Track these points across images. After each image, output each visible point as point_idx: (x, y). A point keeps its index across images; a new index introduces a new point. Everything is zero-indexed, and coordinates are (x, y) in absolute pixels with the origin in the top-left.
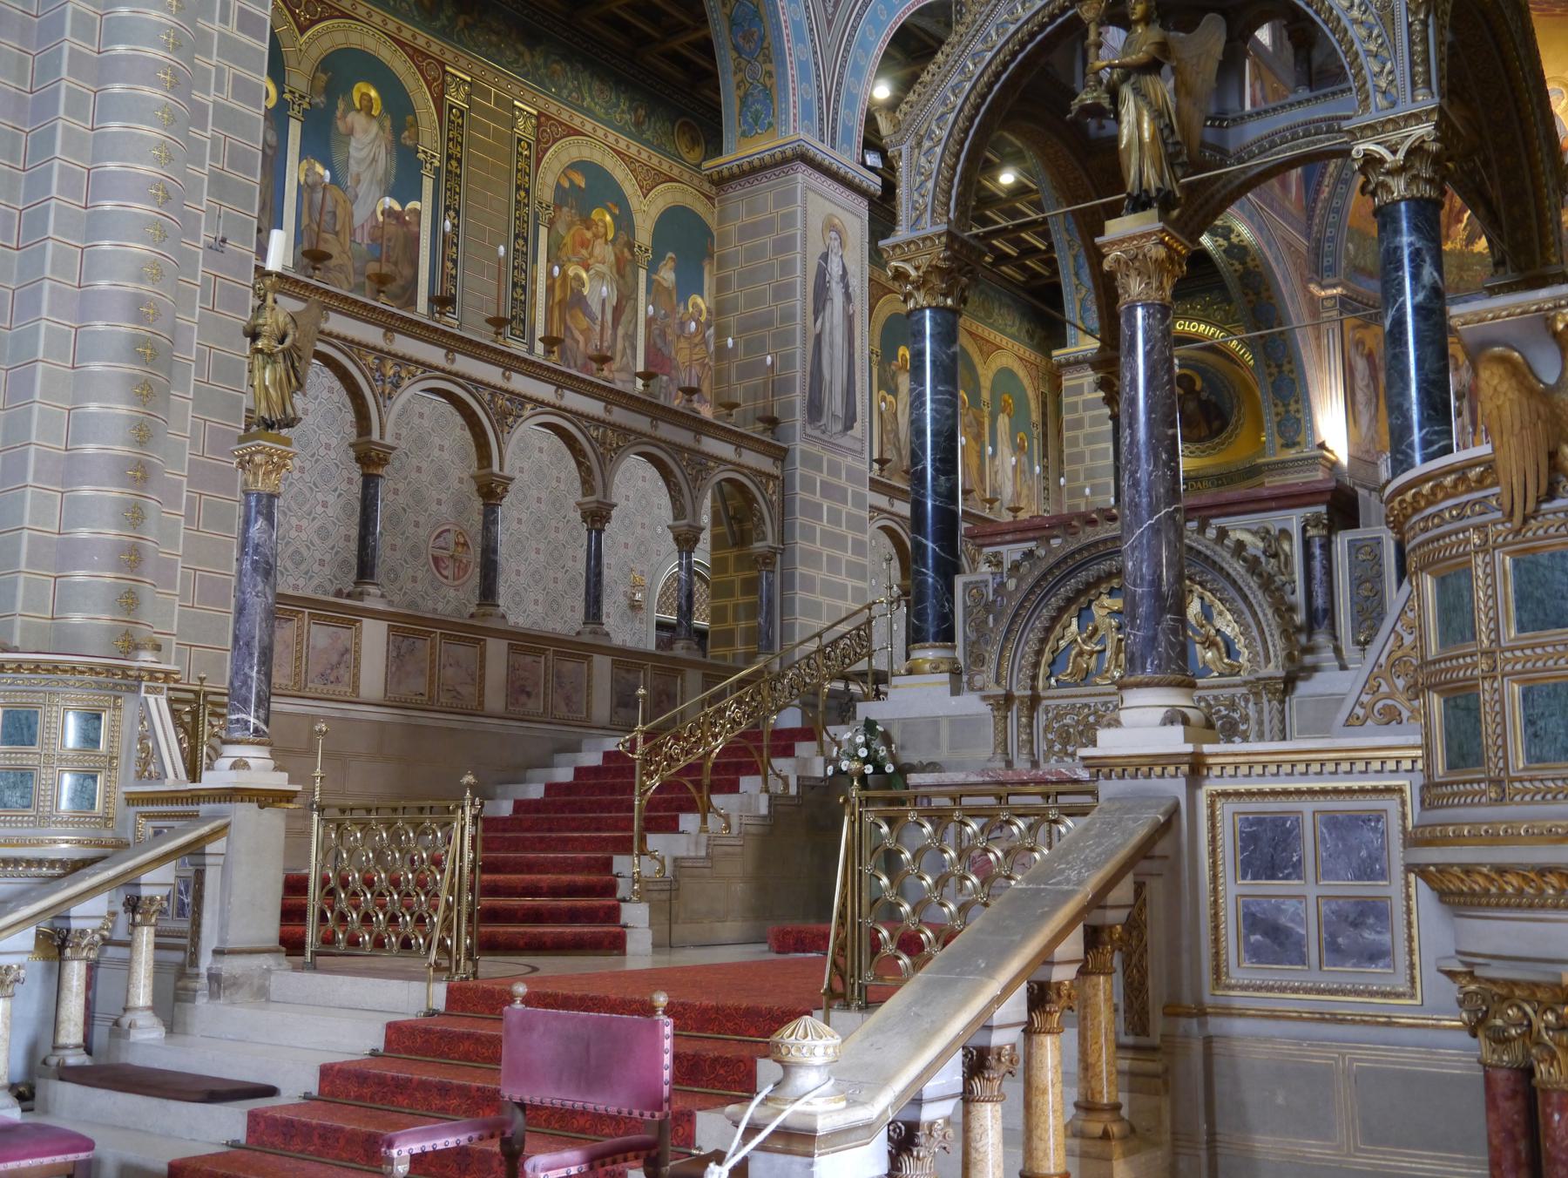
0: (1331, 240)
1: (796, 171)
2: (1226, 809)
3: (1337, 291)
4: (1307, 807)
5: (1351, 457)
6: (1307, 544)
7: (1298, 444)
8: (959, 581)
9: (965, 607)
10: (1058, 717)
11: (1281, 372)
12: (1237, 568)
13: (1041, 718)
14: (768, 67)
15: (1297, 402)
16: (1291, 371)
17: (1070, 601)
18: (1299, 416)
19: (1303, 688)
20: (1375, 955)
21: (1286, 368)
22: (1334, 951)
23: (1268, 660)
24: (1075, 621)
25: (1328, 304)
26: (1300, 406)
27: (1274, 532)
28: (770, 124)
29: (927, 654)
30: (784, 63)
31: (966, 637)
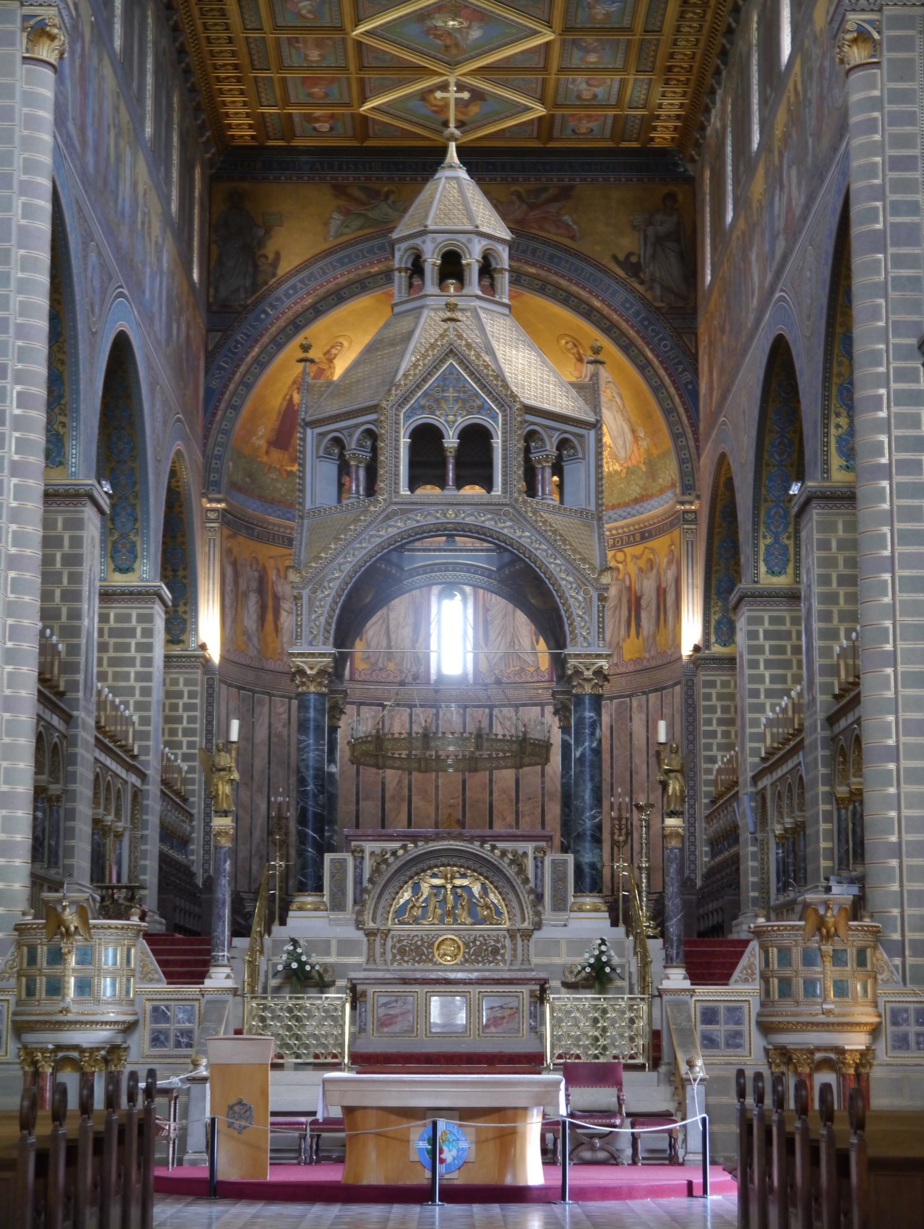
0: (219, 458)
1: (84, 505)
2: (698, 1004)
3: (222, 506)
4: (722, 1005)
5: (223, 658)
6: (535, 858)
7: (182, 642)
8: (328, 857)
9: (331, 873)
10: (399, 941)
11: (175, 576)
12: (511, 872)
13: (389, 943)
14: (61, 418)
15: (185, 604)
16: (185, 577)
17: (411, 878)
18: (185, 617)
19: (537, 935)
20: (738, 1046)
21: (181, 573)
22: (728, 1045)
23: (523, 920)
24: (410, 890)
25: (212, 515)
26: (187, 609)
27: (520, 852)
28: (61, 463)
29: (309, 899)
30: (77, 420)
31: (331, 890)
